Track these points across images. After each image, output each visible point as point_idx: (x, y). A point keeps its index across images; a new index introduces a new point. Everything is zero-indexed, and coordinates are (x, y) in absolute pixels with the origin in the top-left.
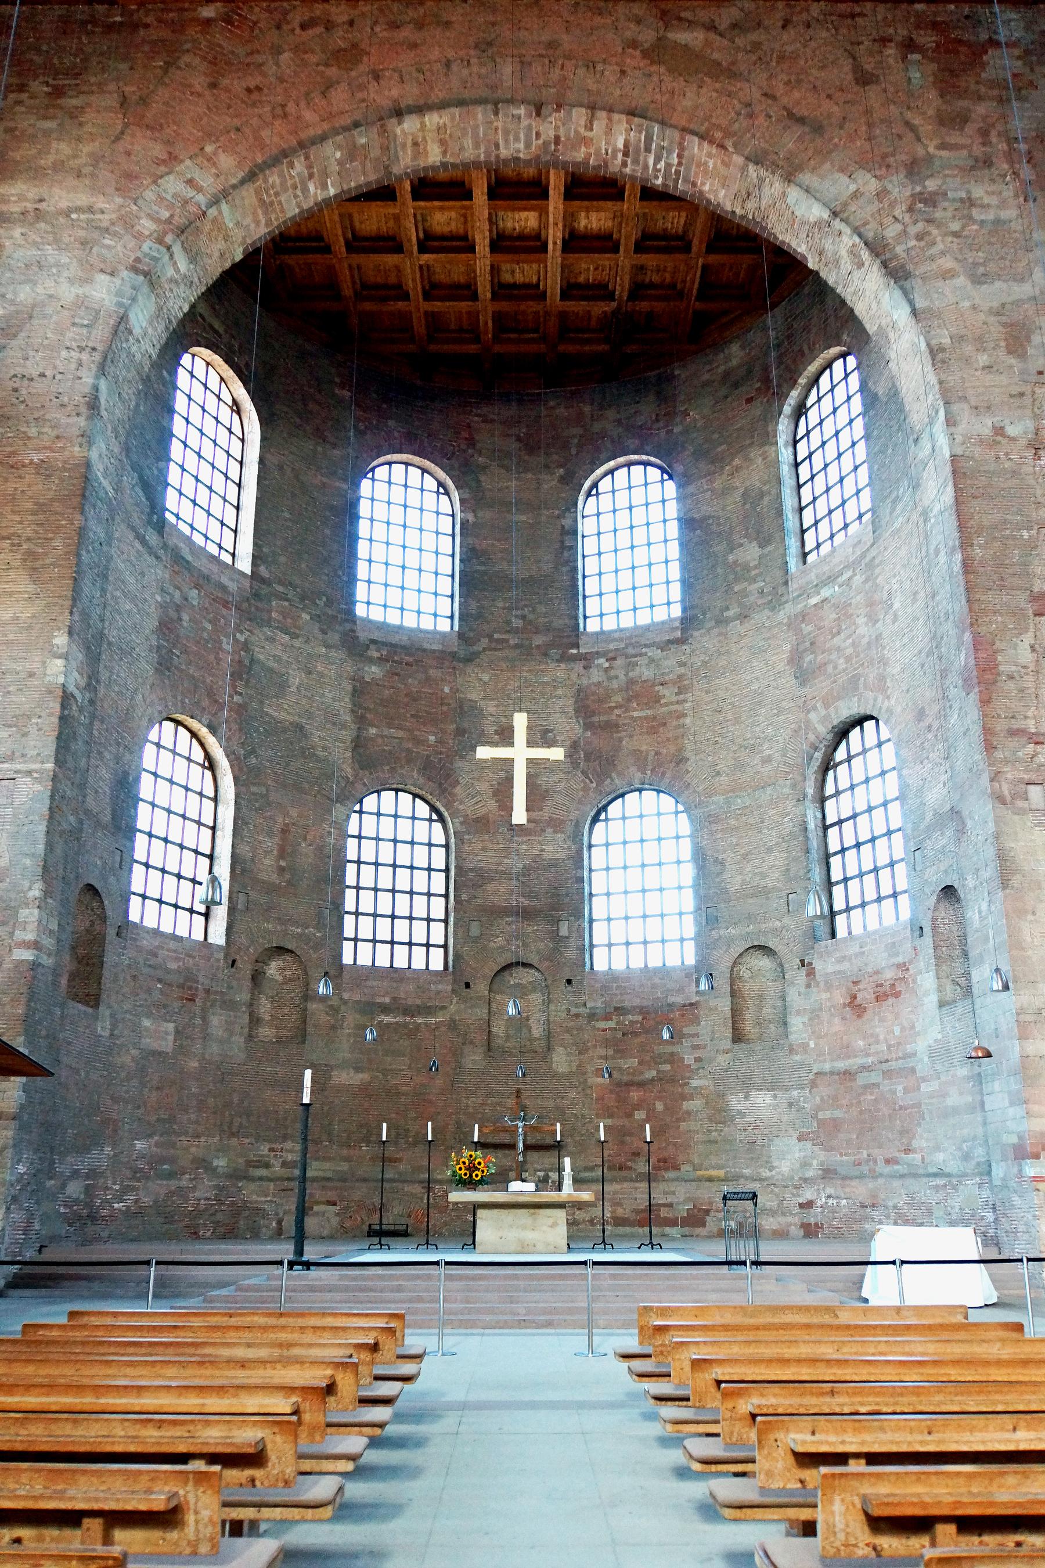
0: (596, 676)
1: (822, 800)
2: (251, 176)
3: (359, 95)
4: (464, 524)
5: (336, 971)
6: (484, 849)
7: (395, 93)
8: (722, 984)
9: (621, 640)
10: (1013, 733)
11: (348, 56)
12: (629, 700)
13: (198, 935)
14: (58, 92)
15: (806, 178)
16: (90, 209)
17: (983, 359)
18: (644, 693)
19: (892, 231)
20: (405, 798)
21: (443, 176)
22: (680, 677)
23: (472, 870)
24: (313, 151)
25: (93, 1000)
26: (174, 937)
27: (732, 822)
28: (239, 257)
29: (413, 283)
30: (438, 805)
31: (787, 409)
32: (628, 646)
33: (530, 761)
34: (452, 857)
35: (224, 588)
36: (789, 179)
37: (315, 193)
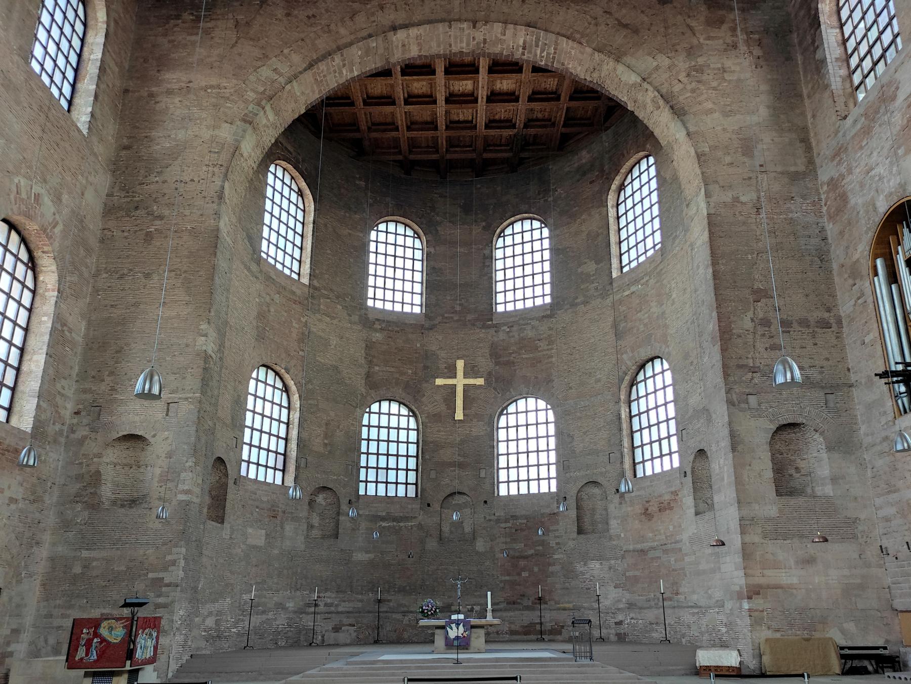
1: (629, 402)
3: (372, 19)
5: (355, 499)
6: (439, 431)
7: (392, 17)
9: (516, 316)
12: (521, 348)
13: (278, 481)
21: (418, 62)
23: (431, 442)
24: (345, 51)
25: (221, 520)
26: (265, 483)
27: (578, 414)
29: (401, 121)
30: (413, 408)
34: (421, 436)
37: (347, 74)
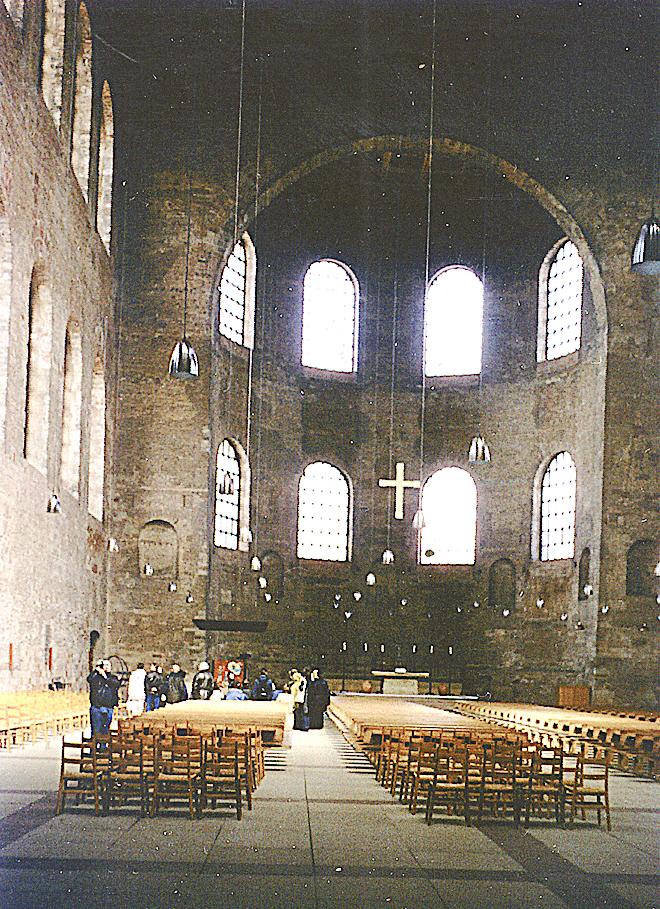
8: (485, 576)
10: (614, 492)
31: (546, 260)
36: (549, 189)
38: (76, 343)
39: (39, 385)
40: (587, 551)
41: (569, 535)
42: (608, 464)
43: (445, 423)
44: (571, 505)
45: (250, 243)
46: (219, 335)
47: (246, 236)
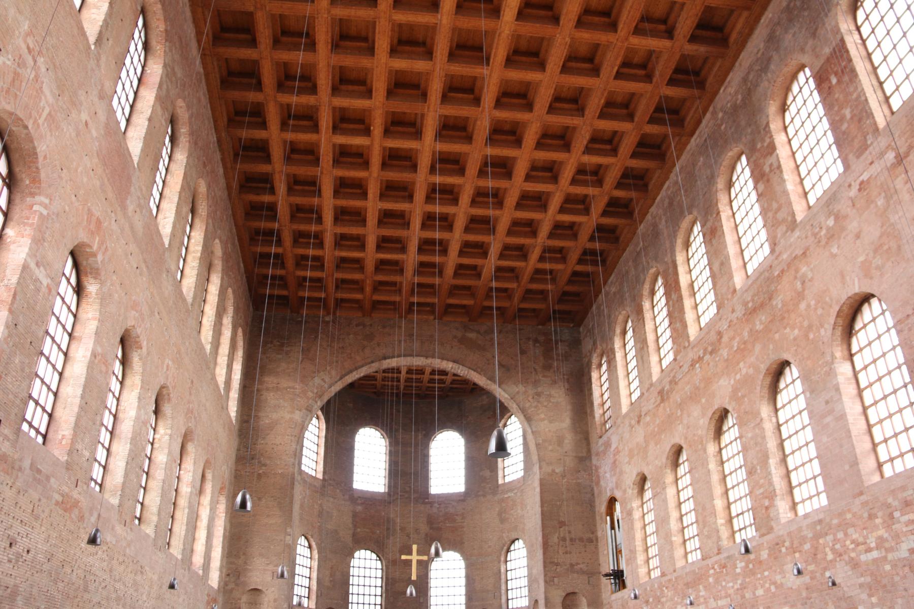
0: (435, 510)
1: (506, 561)
2: (341, 378)
4: (390, 452)
11: (370, 337)
14: (282, 345)
15: (504, 386)
16: (293, 388)
17: (550, 448)
18: (449, 517)
19: (527, 405)
20: (368, 552)
22: (463, 514)
28: (333, 394)
32: (446, 500)
33: (418, 561)
35: (315, 486)
37: (357, 376)
38: (209, 476)
39: (183, 502)
40: (536, 601)
41: (525, 592)
42: (546, 545)
43: (444, 525)
44: (525, 572)
45: (322, 417)
46: (301, 472)
47: (320, 413)
